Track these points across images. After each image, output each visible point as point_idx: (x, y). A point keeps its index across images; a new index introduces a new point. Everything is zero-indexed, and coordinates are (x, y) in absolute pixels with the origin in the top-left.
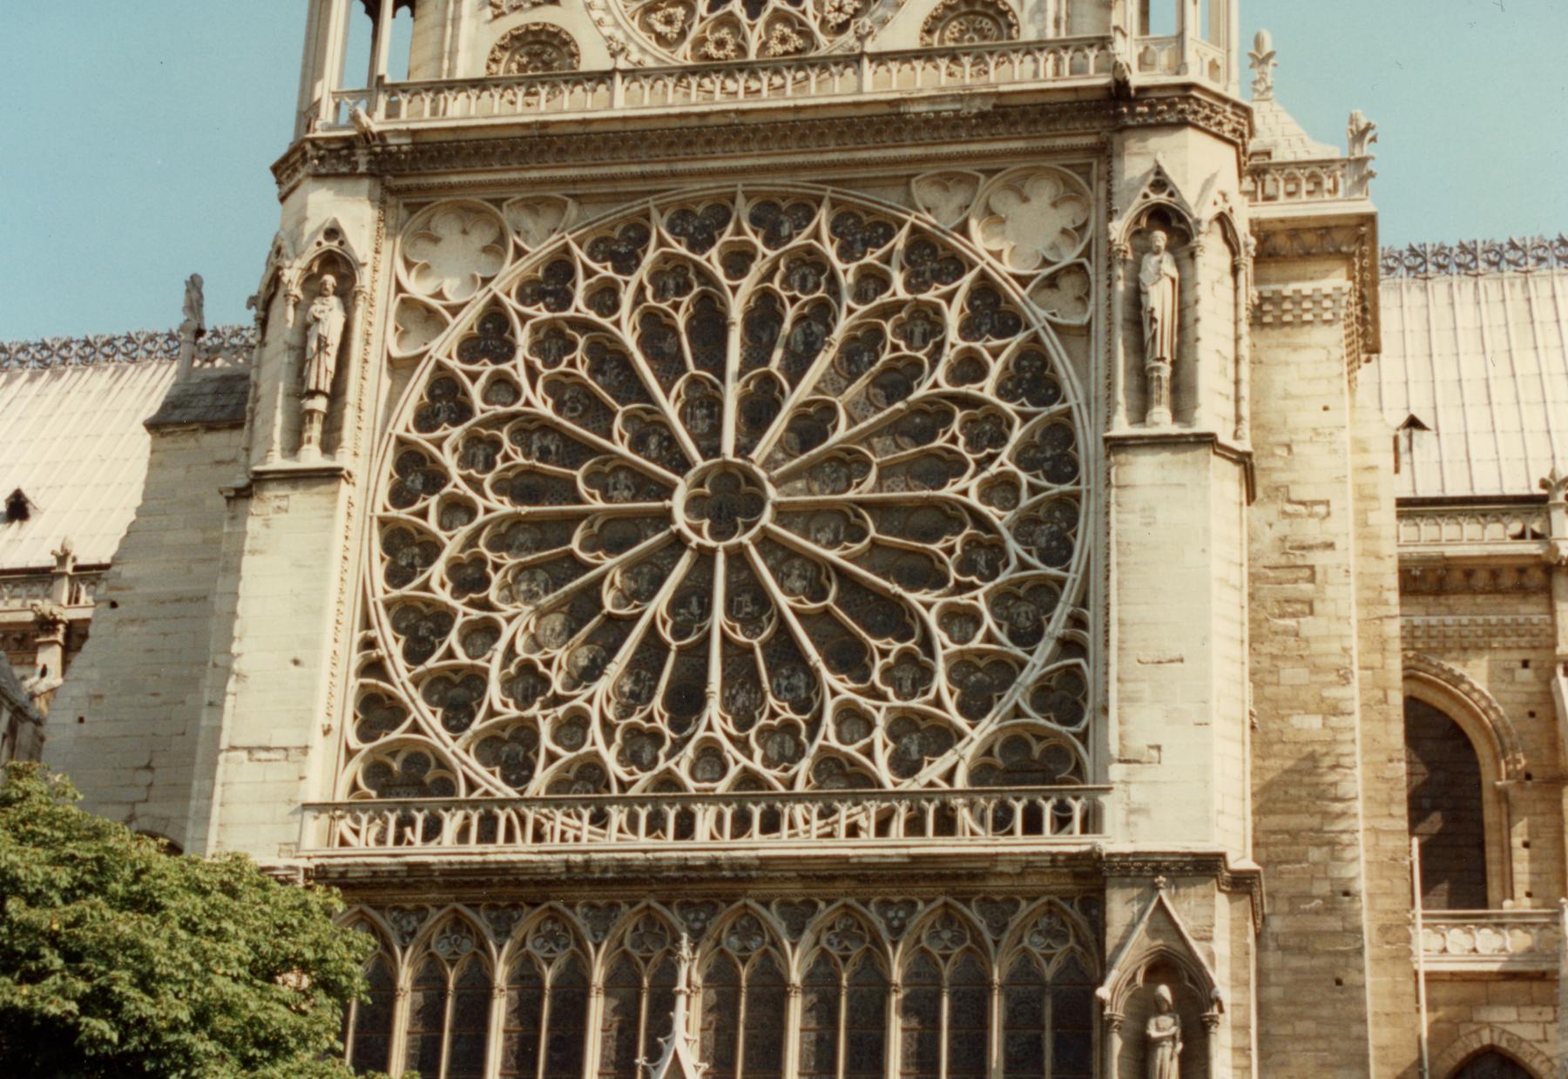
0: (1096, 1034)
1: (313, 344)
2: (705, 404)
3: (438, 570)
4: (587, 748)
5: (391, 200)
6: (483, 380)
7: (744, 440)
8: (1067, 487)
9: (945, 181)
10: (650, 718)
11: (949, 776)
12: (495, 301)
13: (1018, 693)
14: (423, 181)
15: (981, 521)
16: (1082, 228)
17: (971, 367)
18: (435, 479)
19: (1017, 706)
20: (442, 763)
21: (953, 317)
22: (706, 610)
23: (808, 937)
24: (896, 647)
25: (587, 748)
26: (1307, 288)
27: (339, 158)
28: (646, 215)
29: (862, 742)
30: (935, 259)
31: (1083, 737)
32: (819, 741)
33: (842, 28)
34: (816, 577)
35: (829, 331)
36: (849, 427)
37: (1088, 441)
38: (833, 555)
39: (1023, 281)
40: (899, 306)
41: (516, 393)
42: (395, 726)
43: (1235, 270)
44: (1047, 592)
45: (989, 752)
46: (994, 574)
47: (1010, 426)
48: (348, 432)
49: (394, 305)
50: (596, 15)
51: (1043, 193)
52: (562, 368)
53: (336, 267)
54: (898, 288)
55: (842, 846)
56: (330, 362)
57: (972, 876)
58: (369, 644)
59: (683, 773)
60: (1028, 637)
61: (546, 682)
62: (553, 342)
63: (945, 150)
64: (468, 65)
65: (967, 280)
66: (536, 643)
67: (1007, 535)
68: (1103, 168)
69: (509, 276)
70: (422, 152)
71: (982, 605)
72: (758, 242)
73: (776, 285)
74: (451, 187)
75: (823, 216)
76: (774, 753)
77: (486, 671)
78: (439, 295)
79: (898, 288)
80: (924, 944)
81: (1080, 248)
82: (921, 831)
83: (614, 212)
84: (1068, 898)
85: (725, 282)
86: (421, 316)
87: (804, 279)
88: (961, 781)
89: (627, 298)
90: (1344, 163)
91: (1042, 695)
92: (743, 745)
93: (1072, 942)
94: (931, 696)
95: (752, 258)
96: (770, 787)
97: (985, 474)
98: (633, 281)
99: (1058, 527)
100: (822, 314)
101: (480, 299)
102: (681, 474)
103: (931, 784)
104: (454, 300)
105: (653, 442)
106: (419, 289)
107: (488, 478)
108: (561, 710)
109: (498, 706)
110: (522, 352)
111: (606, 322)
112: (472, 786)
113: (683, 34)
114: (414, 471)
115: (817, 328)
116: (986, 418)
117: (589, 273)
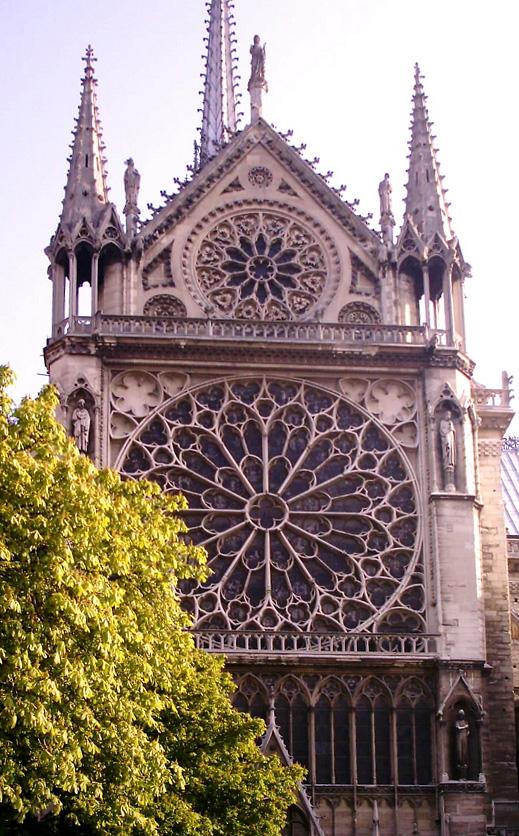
0: (433, 728)
2: (255, 469)
4: (215, 611)
5: (106, 368)
7: (273, 486)
9: (354, 382)
10: (242, 600)
11: (370, 628)
12: (157, 416)
13: (395, 597)
14: (116, 360)
15: (376, 526)
16: (412, 407)
17: (368, 462)
19: (396, 601)
21: (359, 439)
23: (317, 690)
25: (215, 611)
27: (82, 346)
28: (223, 384)
30: (351, 415)
31: (424, 615)
32: (315, 612)
33: (302, 311)
34: (309, 545)
36: (317, 484)
37: (420, 496)
38: (315, 536)
39: (389, 428)
40: (338, 433)
41: (170, 459)
44: (405, 557)
45: (385, 619)
46: (383, 549)
47: (387, 486)
49: (111, 416)
51: (394, 392)
52: (189, 449)
57: (384, 667)
59: (258, 622)
60: (400, 574)
62: (184, 437)
63: (355, 368)
64: (134, 310)
67: (388, 533)
68: (420, 383)
70: (122, 347)
71: (380, 560)
74: (132, 365)
75: (301, 392)
76: (295, 616)
78: (130, 412)
80: (363, 693)
81: (413, 416)
82: (364, 650)
83: (208, 383)
84: (421, 677)
87: (294, 419)
89: (217, 421)
90: (500, 392)
91: (405, 597)
92: (283, 612)
94: (361, 596)
95: (271, 408)
96: (295, 629)
97: (378, 507)
98: (219, 412)
101: (151, 415)
102: (248, 499)
104: (139, 414)
105: (233, 483)
106: (121, 409)
108: (204, 594)
110: (171, 442)
111: (209, 430)
113: (230, 307)
115: (301, 441)
117: (199, 409)
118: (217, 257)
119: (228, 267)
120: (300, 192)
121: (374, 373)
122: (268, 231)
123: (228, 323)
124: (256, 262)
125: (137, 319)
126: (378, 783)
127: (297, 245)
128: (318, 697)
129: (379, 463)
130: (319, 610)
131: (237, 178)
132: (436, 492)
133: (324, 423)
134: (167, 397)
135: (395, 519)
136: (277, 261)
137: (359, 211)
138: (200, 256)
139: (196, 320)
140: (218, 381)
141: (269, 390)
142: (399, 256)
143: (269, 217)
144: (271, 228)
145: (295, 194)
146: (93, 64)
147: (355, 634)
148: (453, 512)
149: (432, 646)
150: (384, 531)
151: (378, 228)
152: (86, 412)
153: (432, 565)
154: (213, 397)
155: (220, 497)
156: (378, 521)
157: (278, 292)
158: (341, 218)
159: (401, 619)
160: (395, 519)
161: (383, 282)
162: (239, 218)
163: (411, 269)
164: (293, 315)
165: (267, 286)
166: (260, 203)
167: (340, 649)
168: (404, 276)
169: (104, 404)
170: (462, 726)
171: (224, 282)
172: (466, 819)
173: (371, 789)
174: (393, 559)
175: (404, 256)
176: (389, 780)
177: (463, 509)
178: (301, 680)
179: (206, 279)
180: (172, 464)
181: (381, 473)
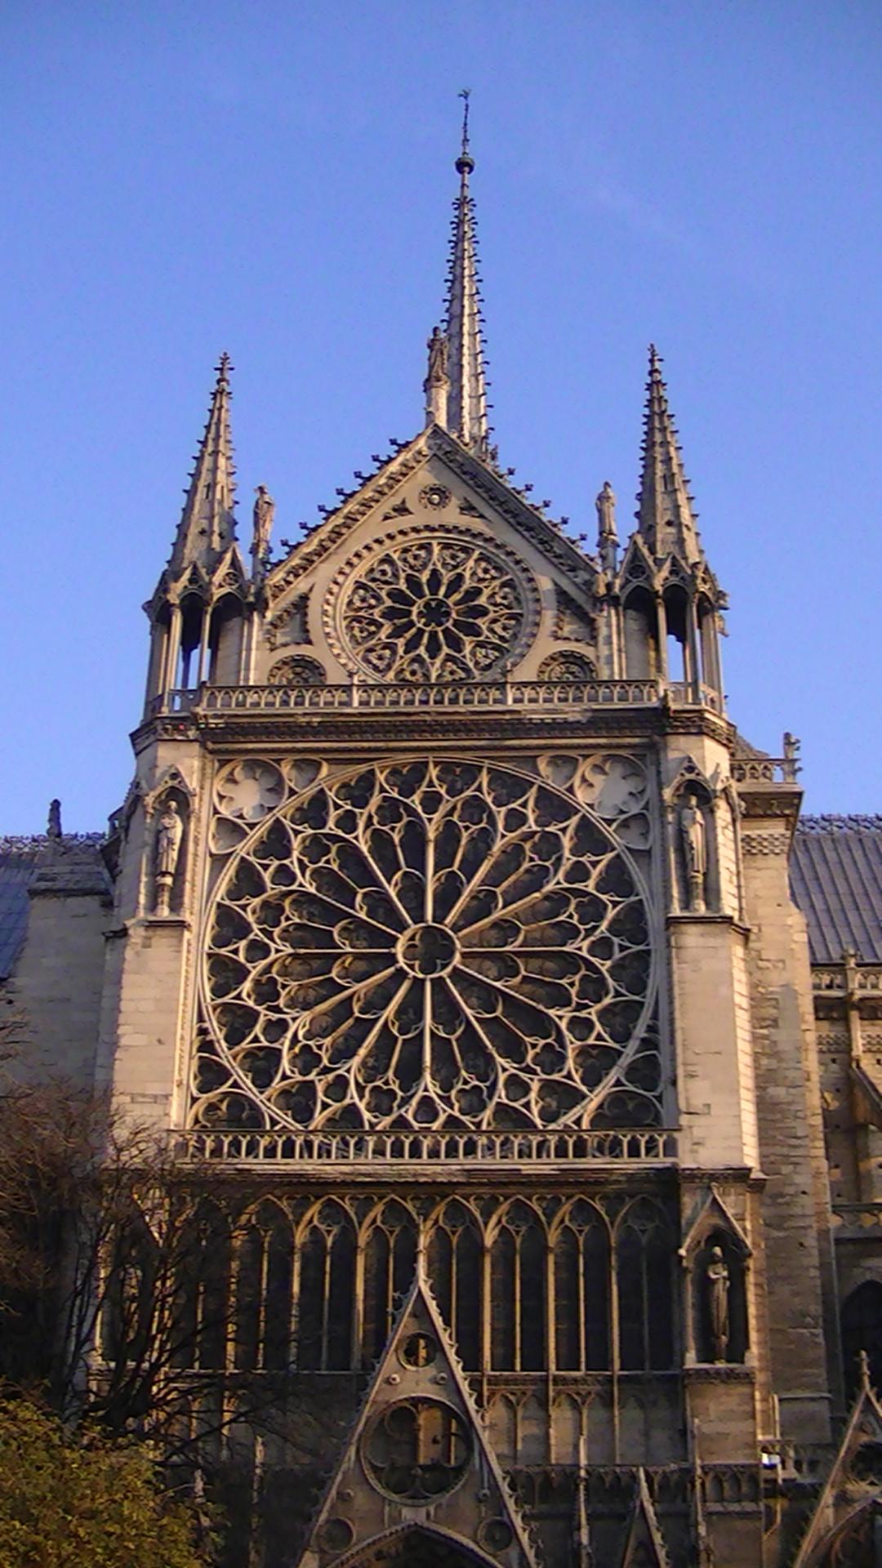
1: (165, 842)
2: (413, 891)
3: (247, 986)
4: (347, 1101)
6: (271, 869)
8: (641, 947)
10: (387, 1083)
11: (578, 1122)
15: (590, 966)
16: (642, 792)
17: (579, 873)
18: (244, 930)
20: (253, 1106)
21: (566, 842)
22: (420, 1016)
24: (542, 1042)
26: (765, 833)
29: (524, 1101)
30: (555, 807)
31: (659, 1098)
32: (496, 1099)
34: (487, 997)
35: (490, 848)
36: (504, 907)
38: (498, 984)
39: (609, 822)
41: (293, 878)
42: (222, 1084)
43: (734, 821)
44: (631, 1011)
46: (599, 1001)
48: (186, 900)
50: (336, 651)
53: (178, 798)
54: (532, 825)
55: (514, 1163)
56: (175, 855)
58: (203, 1032)
59: (410, 1117)
60: (623, 1037)
61: (319, 1058)
62: (316, 848)
65: (575, 820)
66: (309, 1036)
67: (607, 975)
69: (286, 808)
71: (594, 1018)
72: (443, 791)
73: (455, 819)
75: (484, 778)
77: (280, 1051)
78: (241, 817)
79: (532, 825)
81: (643, 803)
85: (424, 816)
86: (231, 829)
87: (472, 815)
88: (585, 1124)
91: (632, 1072)
92: (447, 1100)
93: (657, 1222)
94: (565, 1073)
98: (366, 812)
99: (635, 971)
100: (484, 839)
101: (268, 820)
103: (566, 1126)
105: (381, 911)
106: (226, 812)
107: (277, 931)
108: (331, 1077)
109: (288, 1073)
110: (295, 854)
112: (274, 1122)
113: (389, 667)
114: (229, 925)
115: (481, 845)
116: (590, 901)
118: (373, 602)
119: (389, 614)
120: (488, 513)
121: (587, 747)
122: (444, 565)
123: (382, 688)
124: (427, 605)
125: (256, 689)
126: (588, 1369)
127: (484, 580)
128: (496, 1232)
129: (595, 873)
130: (501, 1095)
131: (404, 502)
132: (676, 911)
133: (516, 819)
134: (292, 792)
135: (617, 955)
136: (456, 604)
137: (566, 532)
138: (350, 603)
139: (338, 687)
140: (363, 768)
141: (438, 778)
142: (622, 587)
143: (446, 546)
144: (449, 561)
145: (481, 516)
146: (228, 375)
147: (554, 1131)
148: (701, 941)
149: (671, 1148)
150: (600, 973)
151: (594, 552)
152: (178, 818)
153: (672, 1021)
154: (358, 793)
155: (362, 931)
156: (592, 959)
157: (457, 645)
158: (542, 542)
159: (625, 1104)
160: (617, 955)
161: (601, 622)
162: (405, 551)
163: (640, 602)
164: (476, 672)
165: (441, 636)
166: (433, 530)
167: (530, 1156)
168: (630, 612)
169: (201, 807)
170: (719, 1273)
171: (383, 635)
172: (721, 1428)
173: (575, 1381)
174: (615, 1014)
175: (630, 587)
176: (606, 1364)
177: (714, 935)
178: (472, 1206)
179: (356, 632)
180: (294, 887)
181: (598, 887)
